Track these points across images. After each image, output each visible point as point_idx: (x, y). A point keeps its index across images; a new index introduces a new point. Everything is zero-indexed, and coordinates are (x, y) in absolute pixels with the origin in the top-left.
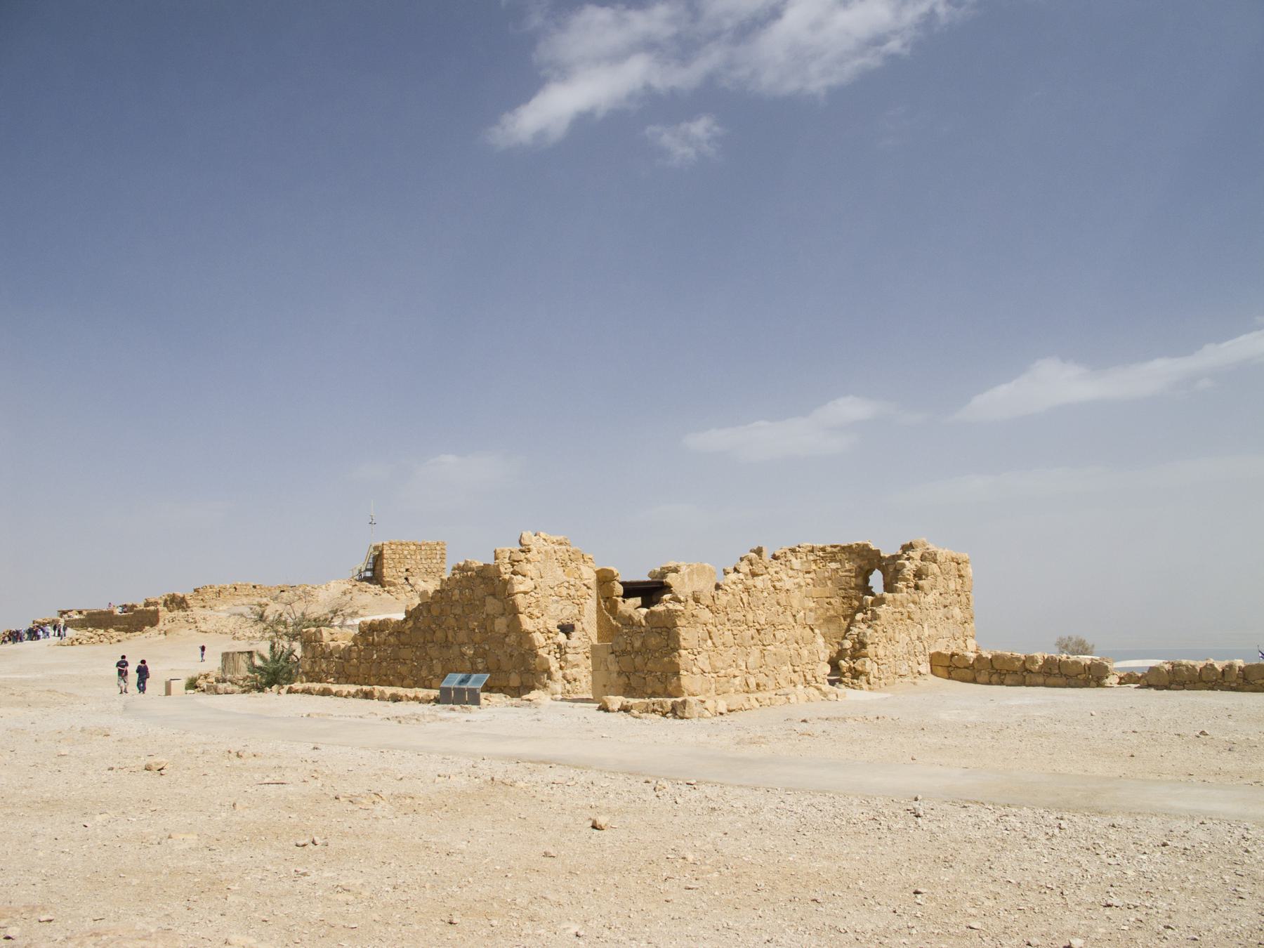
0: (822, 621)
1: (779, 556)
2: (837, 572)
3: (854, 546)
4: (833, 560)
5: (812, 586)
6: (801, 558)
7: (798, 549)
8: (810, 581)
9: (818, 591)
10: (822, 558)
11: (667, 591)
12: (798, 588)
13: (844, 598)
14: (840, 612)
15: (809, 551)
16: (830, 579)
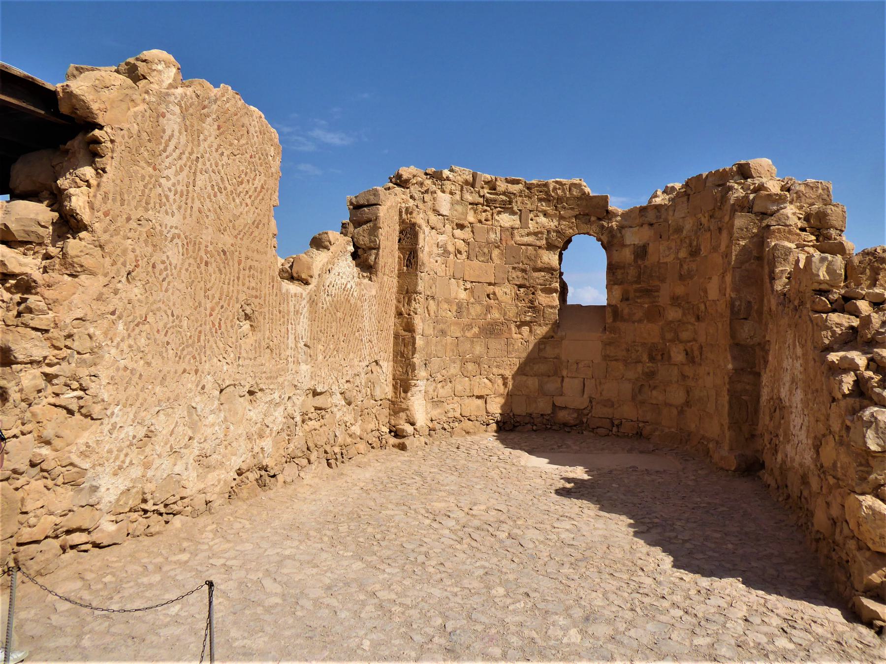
0: (476, 330)
1: (407, 181)
2: (512, 234)
3: (551, 188)
4: (507, 207)
5: (465, 255)
6: (451, 193)
7: (446, 173)
8: (461, 245)
9: (476, 269)
10: (488, 202)
11: (75, 144)
13: (520, 286)
14: (511, 314)
15: (466, 182)
16: (498, 247)
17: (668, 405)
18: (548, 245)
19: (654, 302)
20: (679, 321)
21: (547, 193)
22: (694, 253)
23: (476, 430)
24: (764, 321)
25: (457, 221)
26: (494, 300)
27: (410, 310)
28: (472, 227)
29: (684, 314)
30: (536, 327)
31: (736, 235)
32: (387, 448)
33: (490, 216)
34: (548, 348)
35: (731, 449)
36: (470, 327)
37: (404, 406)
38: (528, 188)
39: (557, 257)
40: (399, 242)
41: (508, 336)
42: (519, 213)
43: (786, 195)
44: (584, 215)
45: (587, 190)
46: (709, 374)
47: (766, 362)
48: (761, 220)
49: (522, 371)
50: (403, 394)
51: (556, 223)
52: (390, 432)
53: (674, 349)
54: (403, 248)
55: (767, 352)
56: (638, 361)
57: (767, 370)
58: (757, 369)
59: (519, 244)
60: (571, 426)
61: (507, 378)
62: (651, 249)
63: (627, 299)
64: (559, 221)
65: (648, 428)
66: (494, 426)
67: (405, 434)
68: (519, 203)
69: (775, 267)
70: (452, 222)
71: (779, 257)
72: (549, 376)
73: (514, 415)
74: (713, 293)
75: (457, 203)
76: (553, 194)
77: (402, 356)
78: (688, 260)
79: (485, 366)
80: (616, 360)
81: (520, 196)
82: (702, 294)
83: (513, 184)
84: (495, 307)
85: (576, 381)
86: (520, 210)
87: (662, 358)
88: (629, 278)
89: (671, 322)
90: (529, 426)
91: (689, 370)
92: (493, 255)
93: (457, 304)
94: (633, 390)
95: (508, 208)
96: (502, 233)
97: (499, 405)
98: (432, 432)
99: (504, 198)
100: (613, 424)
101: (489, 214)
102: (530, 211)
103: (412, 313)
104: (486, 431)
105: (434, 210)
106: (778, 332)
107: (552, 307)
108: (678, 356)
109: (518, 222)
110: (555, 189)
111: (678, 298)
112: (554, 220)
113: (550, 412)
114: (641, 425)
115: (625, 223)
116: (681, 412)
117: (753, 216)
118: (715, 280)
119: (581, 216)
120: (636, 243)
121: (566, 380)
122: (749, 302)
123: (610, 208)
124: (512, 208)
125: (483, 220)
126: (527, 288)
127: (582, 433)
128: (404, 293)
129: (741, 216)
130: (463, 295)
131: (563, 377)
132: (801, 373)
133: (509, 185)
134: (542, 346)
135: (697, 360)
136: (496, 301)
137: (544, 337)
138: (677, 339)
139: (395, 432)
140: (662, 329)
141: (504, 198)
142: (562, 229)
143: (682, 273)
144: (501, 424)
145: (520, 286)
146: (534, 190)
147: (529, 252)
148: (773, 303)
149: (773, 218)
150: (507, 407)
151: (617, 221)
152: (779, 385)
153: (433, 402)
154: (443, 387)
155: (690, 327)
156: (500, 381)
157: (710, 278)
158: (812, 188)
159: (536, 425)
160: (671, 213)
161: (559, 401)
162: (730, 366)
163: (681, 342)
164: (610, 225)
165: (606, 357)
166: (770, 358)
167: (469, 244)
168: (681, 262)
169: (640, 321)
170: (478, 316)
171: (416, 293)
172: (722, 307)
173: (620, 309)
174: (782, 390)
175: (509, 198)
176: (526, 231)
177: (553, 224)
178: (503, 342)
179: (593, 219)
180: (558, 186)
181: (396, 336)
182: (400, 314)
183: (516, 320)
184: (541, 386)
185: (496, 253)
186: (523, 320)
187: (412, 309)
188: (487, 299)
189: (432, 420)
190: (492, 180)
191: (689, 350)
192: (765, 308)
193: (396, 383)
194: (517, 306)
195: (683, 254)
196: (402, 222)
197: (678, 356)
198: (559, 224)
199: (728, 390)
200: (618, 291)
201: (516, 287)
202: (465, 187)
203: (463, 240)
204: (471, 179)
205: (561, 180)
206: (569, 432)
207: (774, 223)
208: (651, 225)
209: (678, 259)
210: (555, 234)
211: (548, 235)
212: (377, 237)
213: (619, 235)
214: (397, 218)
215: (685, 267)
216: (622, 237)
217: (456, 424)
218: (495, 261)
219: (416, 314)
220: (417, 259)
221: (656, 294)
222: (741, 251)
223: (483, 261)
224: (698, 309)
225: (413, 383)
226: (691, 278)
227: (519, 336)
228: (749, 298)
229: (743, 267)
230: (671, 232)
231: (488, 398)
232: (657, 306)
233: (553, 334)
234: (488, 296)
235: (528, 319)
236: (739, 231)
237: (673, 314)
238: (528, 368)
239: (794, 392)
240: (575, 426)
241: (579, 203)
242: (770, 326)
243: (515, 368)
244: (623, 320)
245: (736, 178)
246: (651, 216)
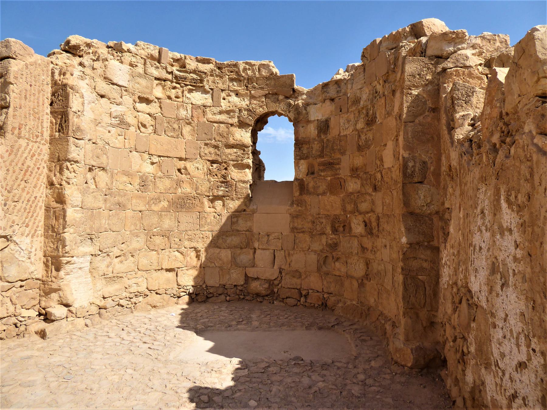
0: (165, 204)
3: (241, 68)
5: (150, 129)
6: (131, 65)
12: (118, 126)
13: (213, 162)
14: (204, 188)
15: (152, 57)
16: (189, 124)
17: (349, 277)
18: (240, 123)
19: (337, 174)
20: (359, 192)
21: (238, 73)
22: (371, 122)
23: (165, 303)
24: (442, 185)
25: (140, 94)
26: (186, 174)
27: (62, 180)
28: (160, 103)
29: (362, 185)
30: (228, 201)
31: (407, 83)
32: (26, 335)
33: (180, 94)
34: (241, 221)
35: (407, 340)
36: (158, 200)
37: (54, 286)
38: (219, 68)
39: (249, 134)
40: (51, 104)
41: (199, 209)
42: (211, 92)
43: (464, 33)
44: (273, 94)
45: (275, 70)
46: (386, 246)
47: (447, 234)
48: (437, 63)
49: (214, 244)
50: (54, 273)
51: (248, 103)
52: (40, 315)
53: (354, 221)
54: (56, 112)
55: (447, 222)
56: (323, 233)
57: (448, 245)
58: (435, 243)
59: (211, 122)
60: (263, 296)
61: (200, 251)
62: (332, 123)
63: (313, 173)
64: (250, 100)
65: (333, 299)
66: (186, 298)
67: (53, 318)
68: (210, 82)
69: (455, 111)
70: (133, 94)
71: (459, 99)
72: (241, 248)
73: (206, 286)
74: (389, 161)
75: (140, 75)
76: (243, 75)
77: (53, 231)
78: (365, 130)
79: (176, 239)
80: (303, 232)
81: (212, 75)
82: (378, 163)
83: (204, 63)
84: (187, 181)
85: (267, 252)
86: (212, 89)
87: (344, 230)
88: (314, 152)
89: (352, 193)
90: (223, 297)
91: (367, 242)
92: (184, 132)
93: (141, 177)
94: (318, 261)
95: (199, 86)
96: (194, 111)
97: (192, 278)
98: (103, 311)
99: (195, 76)
100: (301, 295)
101: (179, 92)
102: (222, 90)
103: (64, 183)
104: (177, 303)
105: (105, 78)
106: (462, 194)
107: (244, 182)
108: (358, 228)
109: (211, 101)
110: (245, 69)
111: (357, 169)
112: (246, 100)
113: (242, 283)
114: (326, 296)
115: (311, 101)
116: (361, 285)
117: (426, 60)
118: (390, 145)
119: (270, 96)
120: (319, 118)
121: (258, 252)
122: (424, 163)
123: (296, 86)
124: (203, 87)
125: (173, 96)
126: (220, 163)
127: (273, 303)
128: (56, 161)
129: (413, 61)
130: (149, 169)
131: (255, 249)
132: (515, 259)
133: (200, 64)
134: (235, 220)
135: (374, 231)
136: (188, 176)
137: (237, 211)
138: (356, 211)
139: (46, 315)
140: (343, 200)
141: (195, 76)
142: (252, 108)
143: (360, 144)
144: (194, 296)
145: (213, 162)
146: (225, 70)
147: (221, 129)
148: (454, 155)
149: (449, 60)
150: (200, 279)
151: (302, 99)
152: (467, 269)
153: (105, 278)
154: (121, 262)
155: (368, 197)
156: (193, 254)
157: (385, 145)
158: (489, 40)
159: (229, 296)
160: (349, 86)
161: (252, 272)
162: (404, 240)
163: (360, 213)
164: (296, 103)
165: (293, 230)
166: (452, 230)
167: (155, 119)
168: (359, 133)
169: (324, 194)
170: (167, 191)
171: (69, 161)
172: (397, 174)
173: (306, 183)
174: (473, 279)
175: (200, 76)
176: (219, 109)
177: (244, 103)
178: (195, 215)
179: (281, 97)
180: (247, 67)
181: (48, 209)
182: (51, 184)
183: (208, 194)
184: (234, 258)
185: (187, 130)
186: (215, 194)
187: (64, 178)
188: (179, 174)
189: (104, 298)
190: (181, 58)
191: (367, 221)
192: (444, 168)
193: (47, 261)
194: (209, 180)
195: (360, 125)
196: (55, 83)
197: (358, 228)
198: (250, 103)
199: (402, 268)
200: (304, 165)
201: (208, 163)
202: (148, 61)
203: (149, 114)
204: (157, 54)
205: (251, 61)
206: (261, 302)
207: (450, 65)
208: (332, 100)
209: (357, 130)
210: (246, 113)
211: (240, 113)
212: (8, 93)
213: (304, 112)
214: (49, 79)
215: (363, 137)
216: (307, 114)
217: (141, 299)
218: (187, 137)
219: (69, 184)
220: (69, 123)
221: (337, 166)
222: (413, 102)
223: (172, 137)
224: (375, 179)
225: (65, 260)
226: (368, 147)
227: (213, 210)
228: (424, 157)
229: (417, 121)
230: (350, 103)
231: (179, 270)
232: (338, 178)
233: (244, 208)
234: (179, 170)
235: (221, 193)
236: (411, 78)
237: (353, 186)
238: (220, 241)
239: (498, 288)
240: (267, 296)
241: (268, 82)
242: (450, 190)
243: (208, 241)
244: (309, 193)
245: (409, 38)
246: (332, 91)
